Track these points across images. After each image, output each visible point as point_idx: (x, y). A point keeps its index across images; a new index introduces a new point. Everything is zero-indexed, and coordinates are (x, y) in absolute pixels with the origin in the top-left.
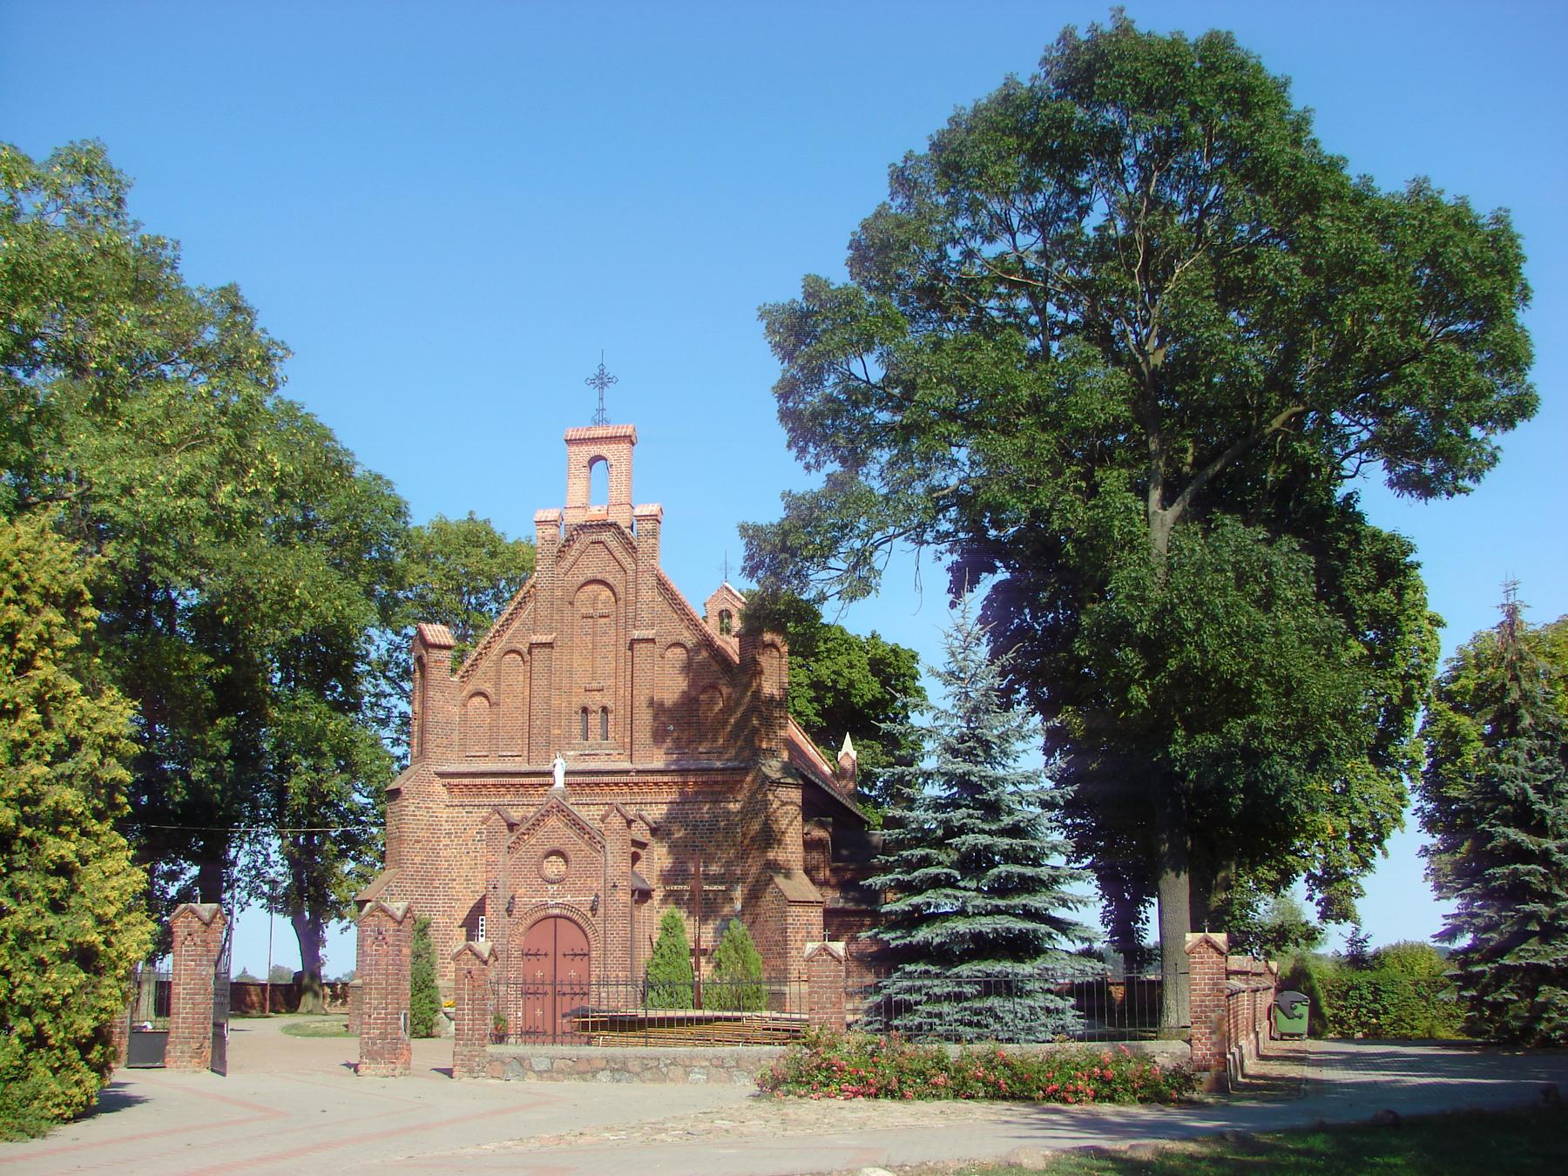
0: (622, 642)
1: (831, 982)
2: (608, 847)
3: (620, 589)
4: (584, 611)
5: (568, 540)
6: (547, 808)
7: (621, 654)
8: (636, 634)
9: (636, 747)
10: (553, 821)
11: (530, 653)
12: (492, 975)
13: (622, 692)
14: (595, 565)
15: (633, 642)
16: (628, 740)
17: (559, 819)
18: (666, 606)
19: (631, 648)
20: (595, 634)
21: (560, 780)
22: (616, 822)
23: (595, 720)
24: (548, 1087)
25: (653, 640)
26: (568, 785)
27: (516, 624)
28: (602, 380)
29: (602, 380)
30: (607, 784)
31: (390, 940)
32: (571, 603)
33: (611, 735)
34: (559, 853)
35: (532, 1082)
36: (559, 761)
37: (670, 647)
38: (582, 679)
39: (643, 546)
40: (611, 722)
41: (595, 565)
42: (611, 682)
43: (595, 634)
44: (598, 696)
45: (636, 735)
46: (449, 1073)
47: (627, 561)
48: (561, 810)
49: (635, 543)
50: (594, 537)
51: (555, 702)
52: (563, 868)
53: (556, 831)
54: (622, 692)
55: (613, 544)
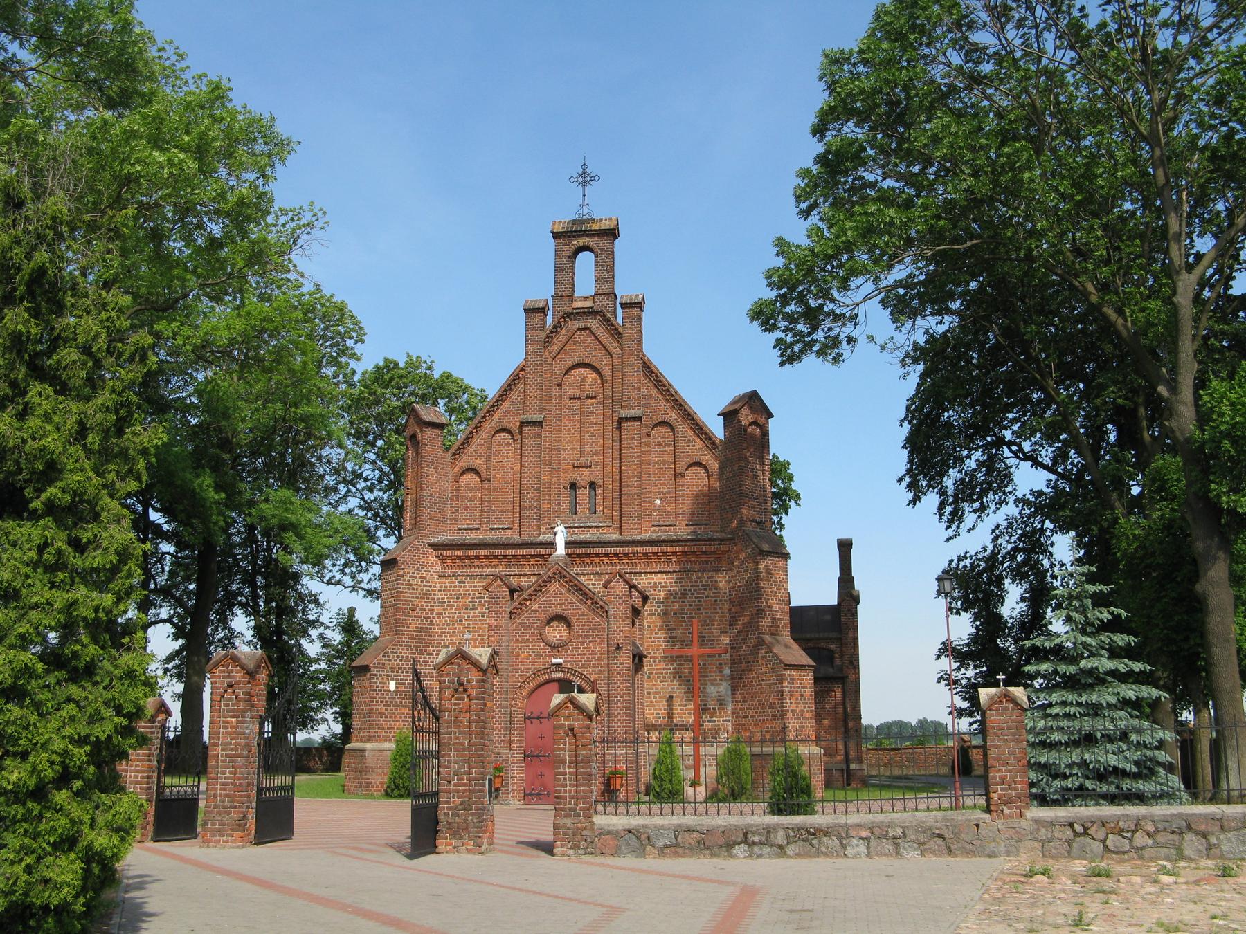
0: (609, 421)
1: (1015, 734)
2: (611, 612)
3: (607, 372)
4: (571, 392)
5: (555, 327)
6: (550, 573)
7: (608, 432)
8: (624, 414)
9: (624, 520)
10: (555, 587)
11: (520, 432)
12: (596, 733)
13: (609, 468)
14: (580, 350)
15: (621, 420)
16: (616, 513)
17: (561, 585)
18: (651, 387)
19: (619, 428)
20: (582, 414)
21: (561, 550)
22: (619, 586)
23: (583, 494)
24: (671, 864)
25: (639, 419)
26: (569, 555)
27: (506, 404)
28: (585, 179)
29: (585, 179)
30: (598, 555)
31: (473, 692)
32: (560, 385)
33: (599, 509)
34: (561, 618)
35: (651, 862)
36: (560, 529)
37: (655, 426)
38: (569, 455)
39: (629, 332)
40: (599, 496)
41: (580, 350)
42: (598, 458)
43: (582, 414)
44: (586, 472)
45: (625, 508)
46: (548, 848)
47: (612, 345)
48: (563, 576)
49: (621, 330)
50: (581, 324)
51: (545, 478)
52: (565, 633)
53: (558, 597)
54: (609, 468)
55: (600, 331)
